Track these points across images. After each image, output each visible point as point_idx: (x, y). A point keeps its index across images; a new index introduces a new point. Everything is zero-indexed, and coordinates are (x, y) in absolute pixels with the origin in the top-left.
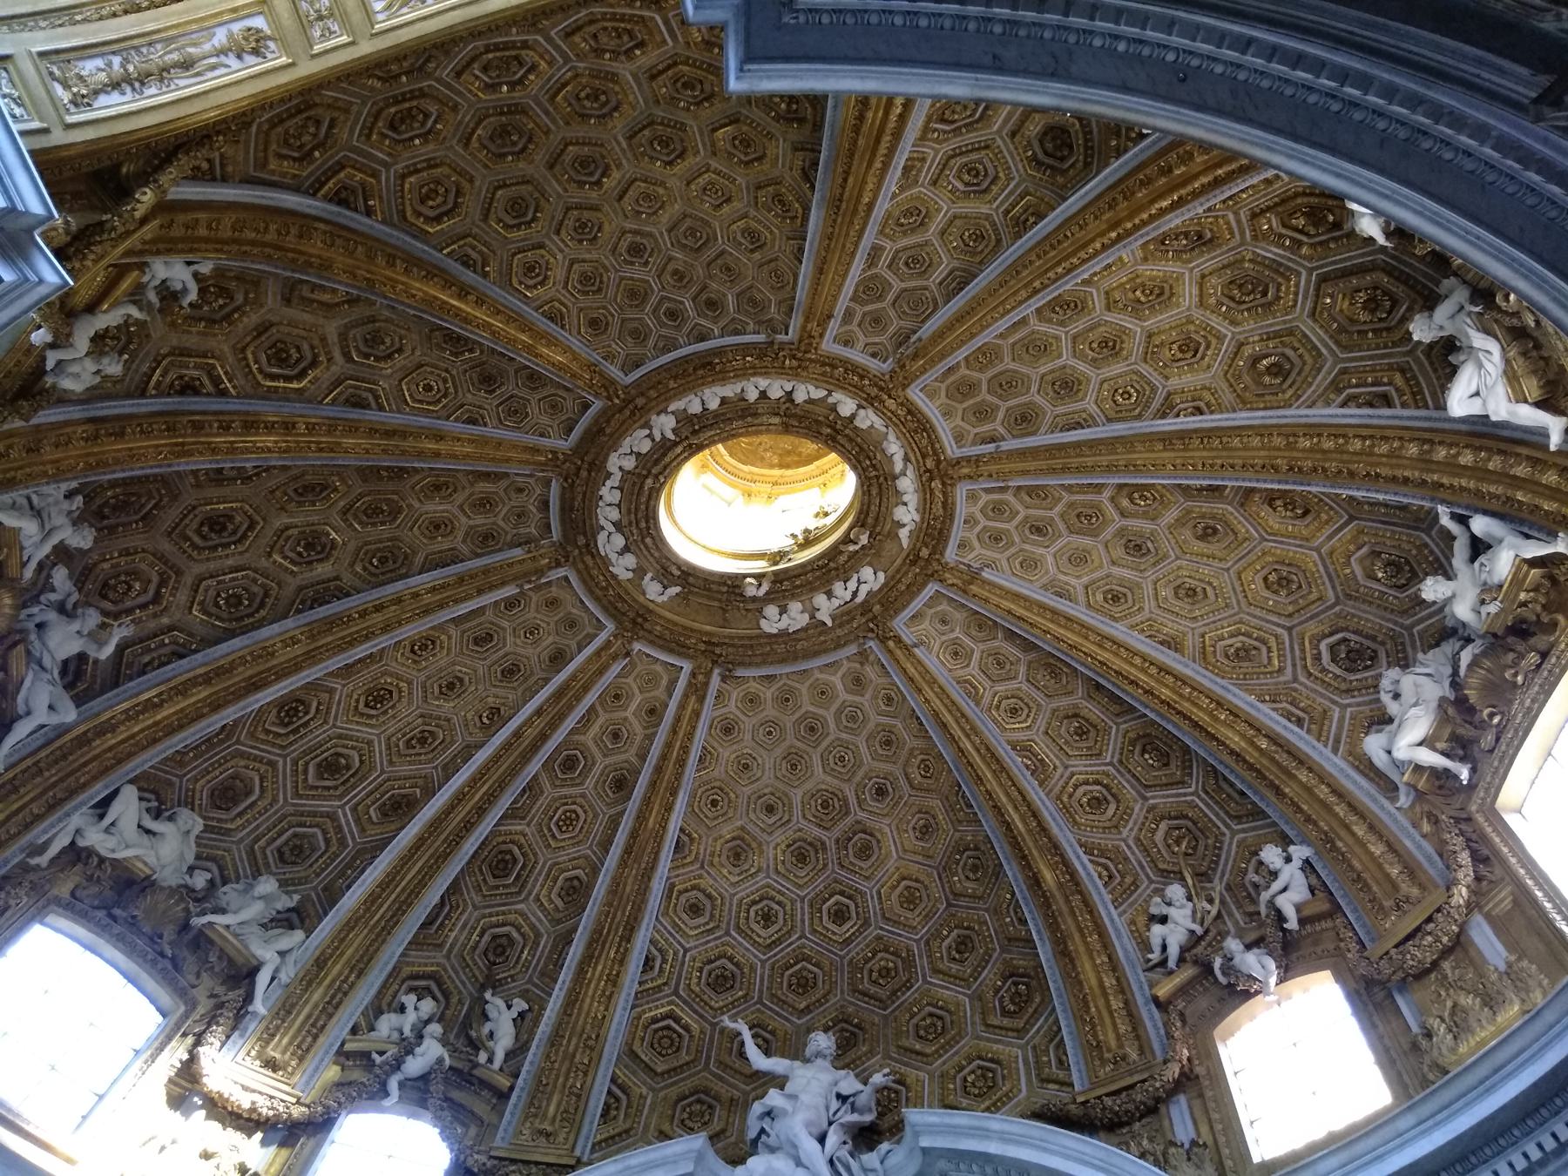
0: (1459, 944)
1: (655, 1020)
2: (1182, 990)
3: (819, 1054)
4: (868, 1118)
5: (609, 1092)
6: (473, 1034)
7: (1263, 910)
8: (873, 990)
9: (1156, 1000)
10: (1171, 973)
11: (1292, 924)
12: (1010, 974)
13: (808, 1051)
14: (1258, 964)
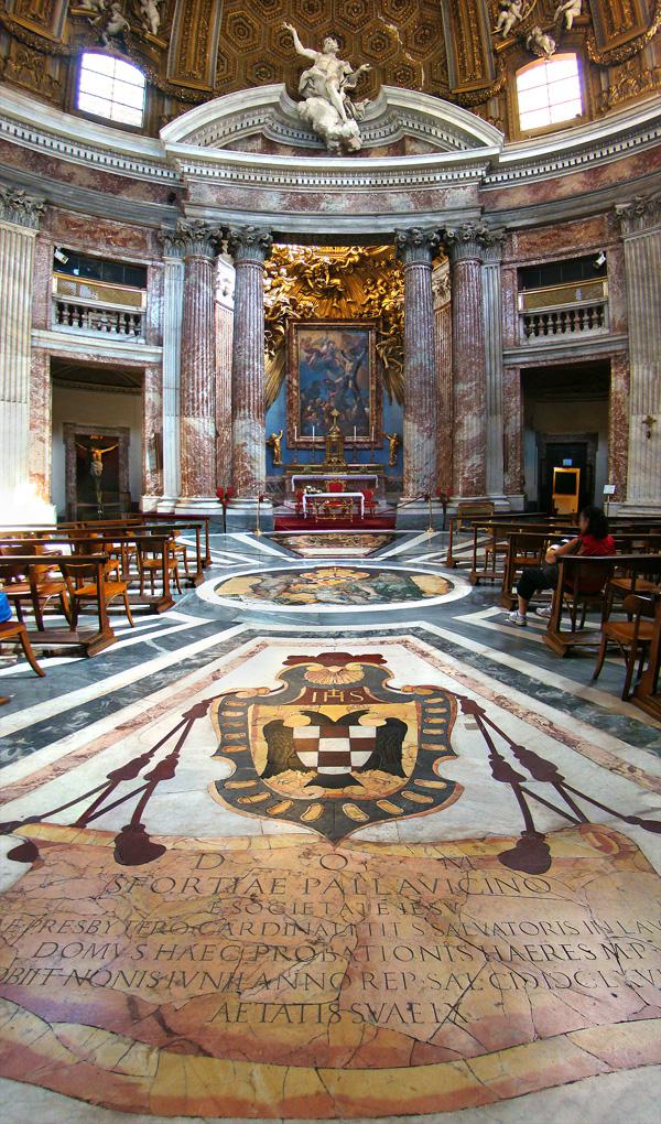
0: (637, 55)
1: (235, 18)
2: (507, 49)
3: (332, 50)
4: (354, 86)
5: (219, 57)
6: (136, 12)
7: (557, 15)
8: (349, 18)
9: (495, 51)
10: (502, 39)
11: (569, 27)
12: (423, 24)
13: (325, 49)
14: (547, 42)
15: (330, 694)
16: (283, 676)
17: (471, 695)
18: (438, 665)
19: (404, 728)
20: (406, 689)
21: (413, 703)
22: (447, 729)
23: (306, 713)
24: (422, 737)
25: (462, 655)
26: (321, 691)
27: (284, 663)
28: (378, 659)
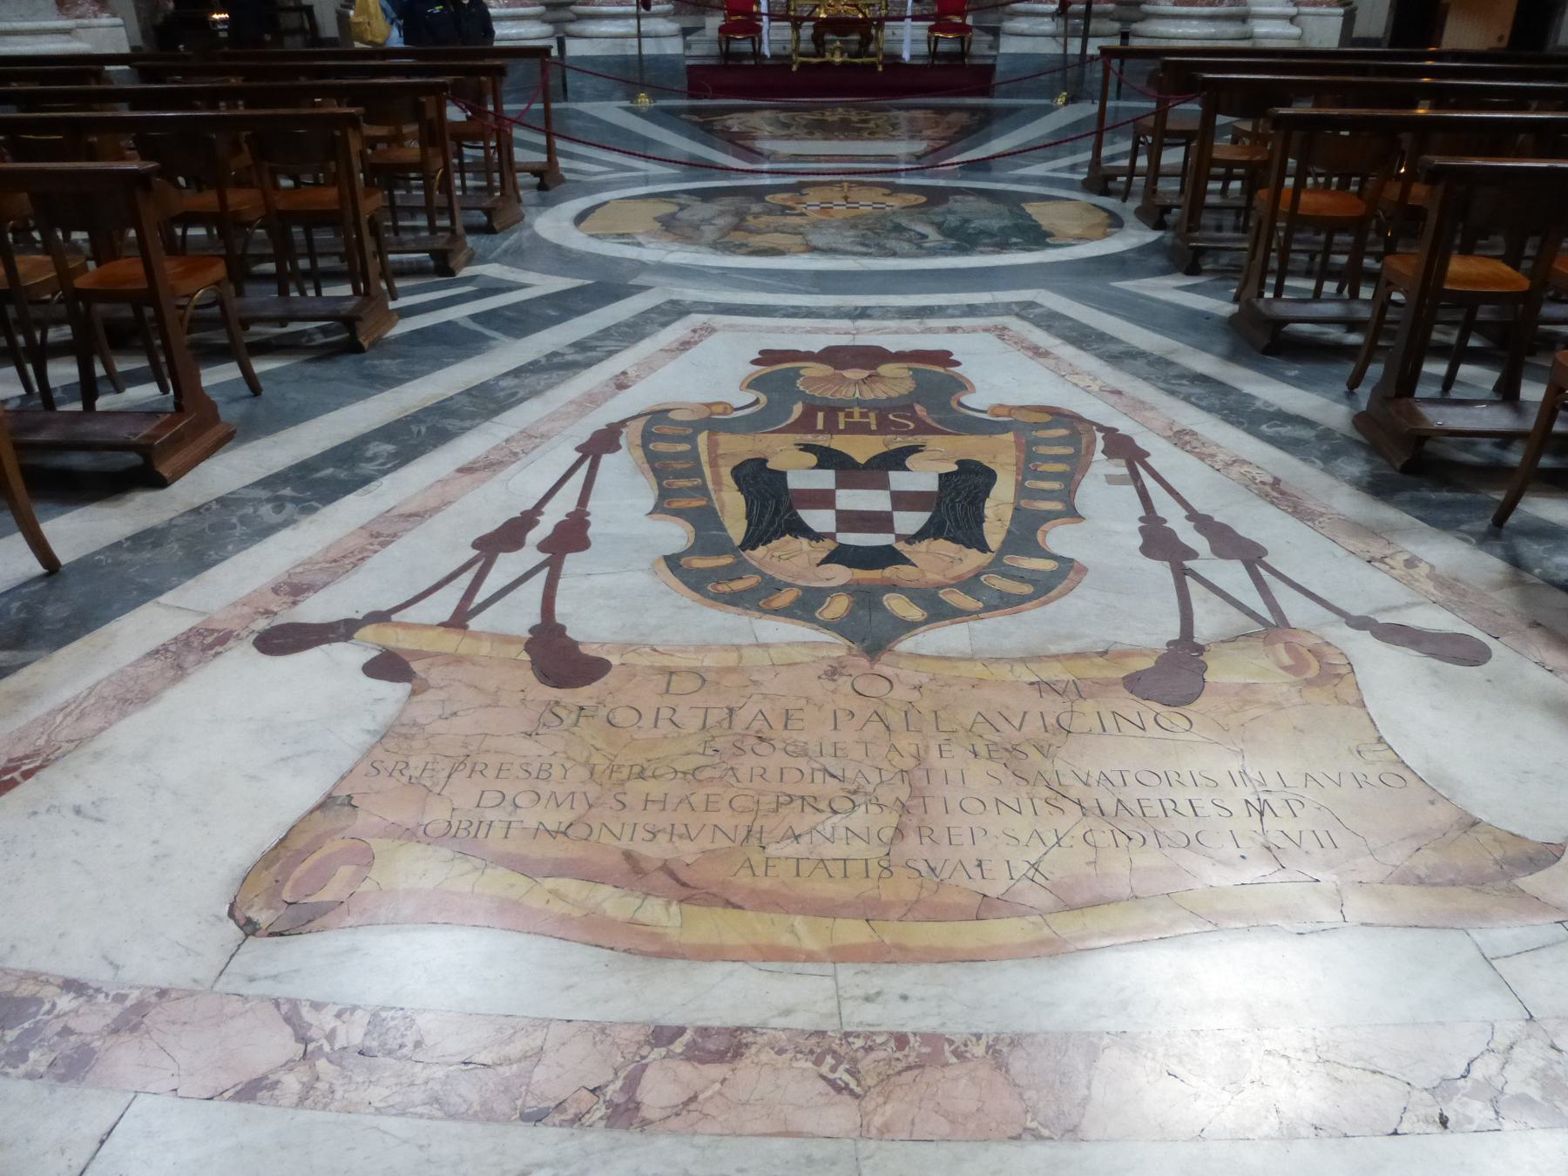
15: (849, 415)
16: (754, 384)
17: (1124, 426)
18: (1063, 372)
19: (990, 476)
20: (998, 411)
21: (1010, 437)
22: (1070, 483)
23: (807, 448)
24: (1021, 491)
25: (1121, 356)
26: (832, 410)
27: (755, 362)
28: (943, 358)
